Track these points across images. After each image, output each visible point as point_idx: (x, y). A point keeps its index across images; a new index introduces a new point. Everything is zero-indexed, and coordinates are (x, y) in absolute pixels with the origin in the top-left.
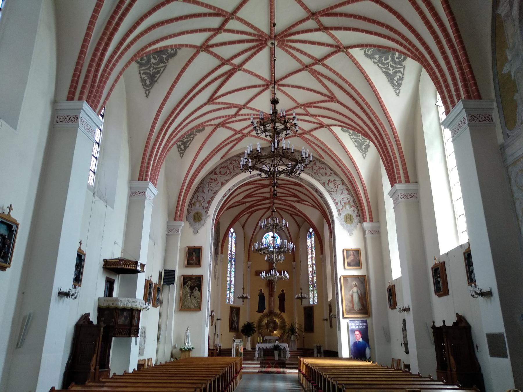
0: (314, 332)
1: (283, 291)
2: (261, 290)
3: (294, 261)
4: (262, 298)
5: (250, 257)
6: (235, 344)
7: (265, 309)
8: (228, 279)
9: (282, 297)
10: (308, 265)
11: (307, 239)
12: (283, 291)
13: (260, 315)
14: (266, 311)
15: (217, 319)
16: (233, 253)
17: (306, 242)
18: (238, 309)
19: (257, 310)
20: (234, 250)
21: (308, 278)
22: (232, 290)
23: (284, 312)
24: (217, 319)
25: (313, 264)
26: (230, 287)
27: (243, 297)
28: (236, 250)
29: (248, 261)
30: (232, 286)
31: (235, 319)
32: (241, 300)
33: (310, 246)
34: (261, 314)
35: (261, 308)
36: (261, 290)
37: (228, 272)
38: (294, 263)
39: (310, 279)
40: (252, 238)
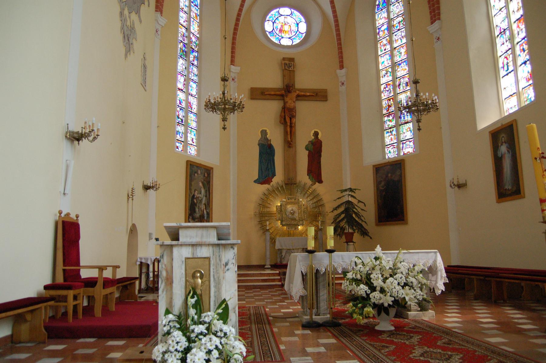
0: (406, 223)
1: (316, 134)
2: (264, 133)
3: (342, 67)
4: (266, 151)
5: (237, 55)
6: (181, 254)
7: (274, 175)
8: (181, 96)
9: (315, 150)
10: (378, 71)
11: (374, 14)
12: (316, 134)
13: (263, 188)
14: (278, 179)
15: (147, 188)
16: (194, 39)
17: (374, 21)
18: (208, 172)
19: (256, 177)
20: (195, 28)
21: (380, 101)
22: (194, 125)
23: (320, 181)
24: (147, 188)
25: (394, 65)
26: (186, 117)
27: (225, 101)
28: (200, 32)
29: (232, 62)
30: (192, 117)
31: (202, 195)
32: (217, 117)
33: (385, 27)
34: (266, 186)
35: (266, 174)
36: (264, 133)
37: (181, 79)
38: (341, 73)
39: (384, 103)
40: (240, 10)
